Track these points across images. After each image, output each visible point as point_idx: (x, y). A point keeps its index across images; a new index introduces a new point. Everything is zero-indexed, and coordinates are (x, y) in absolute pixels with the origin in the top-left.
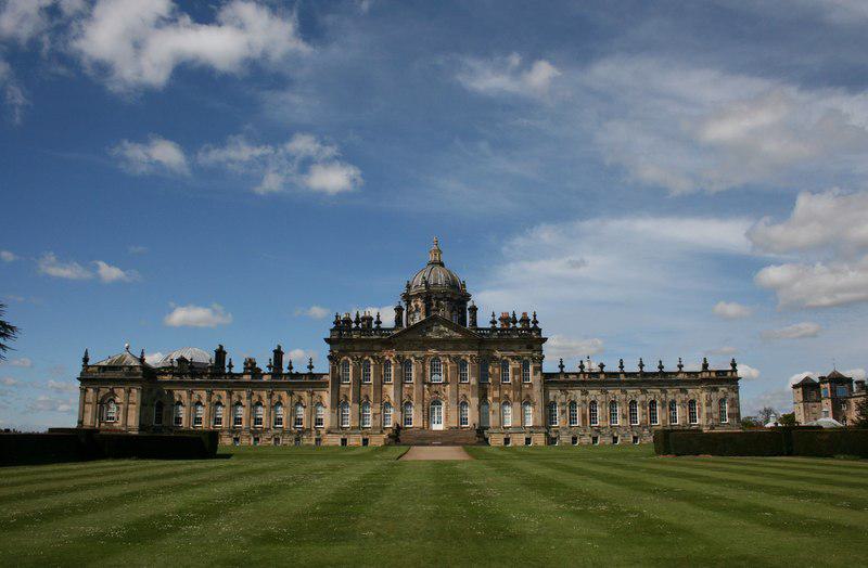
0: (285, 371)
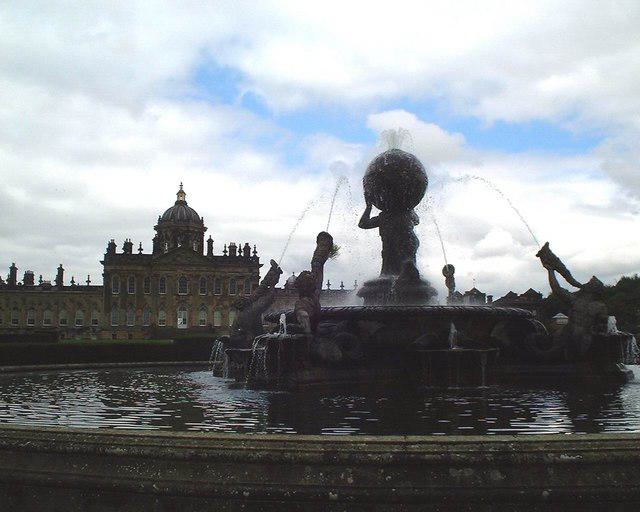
0: (67, 283)
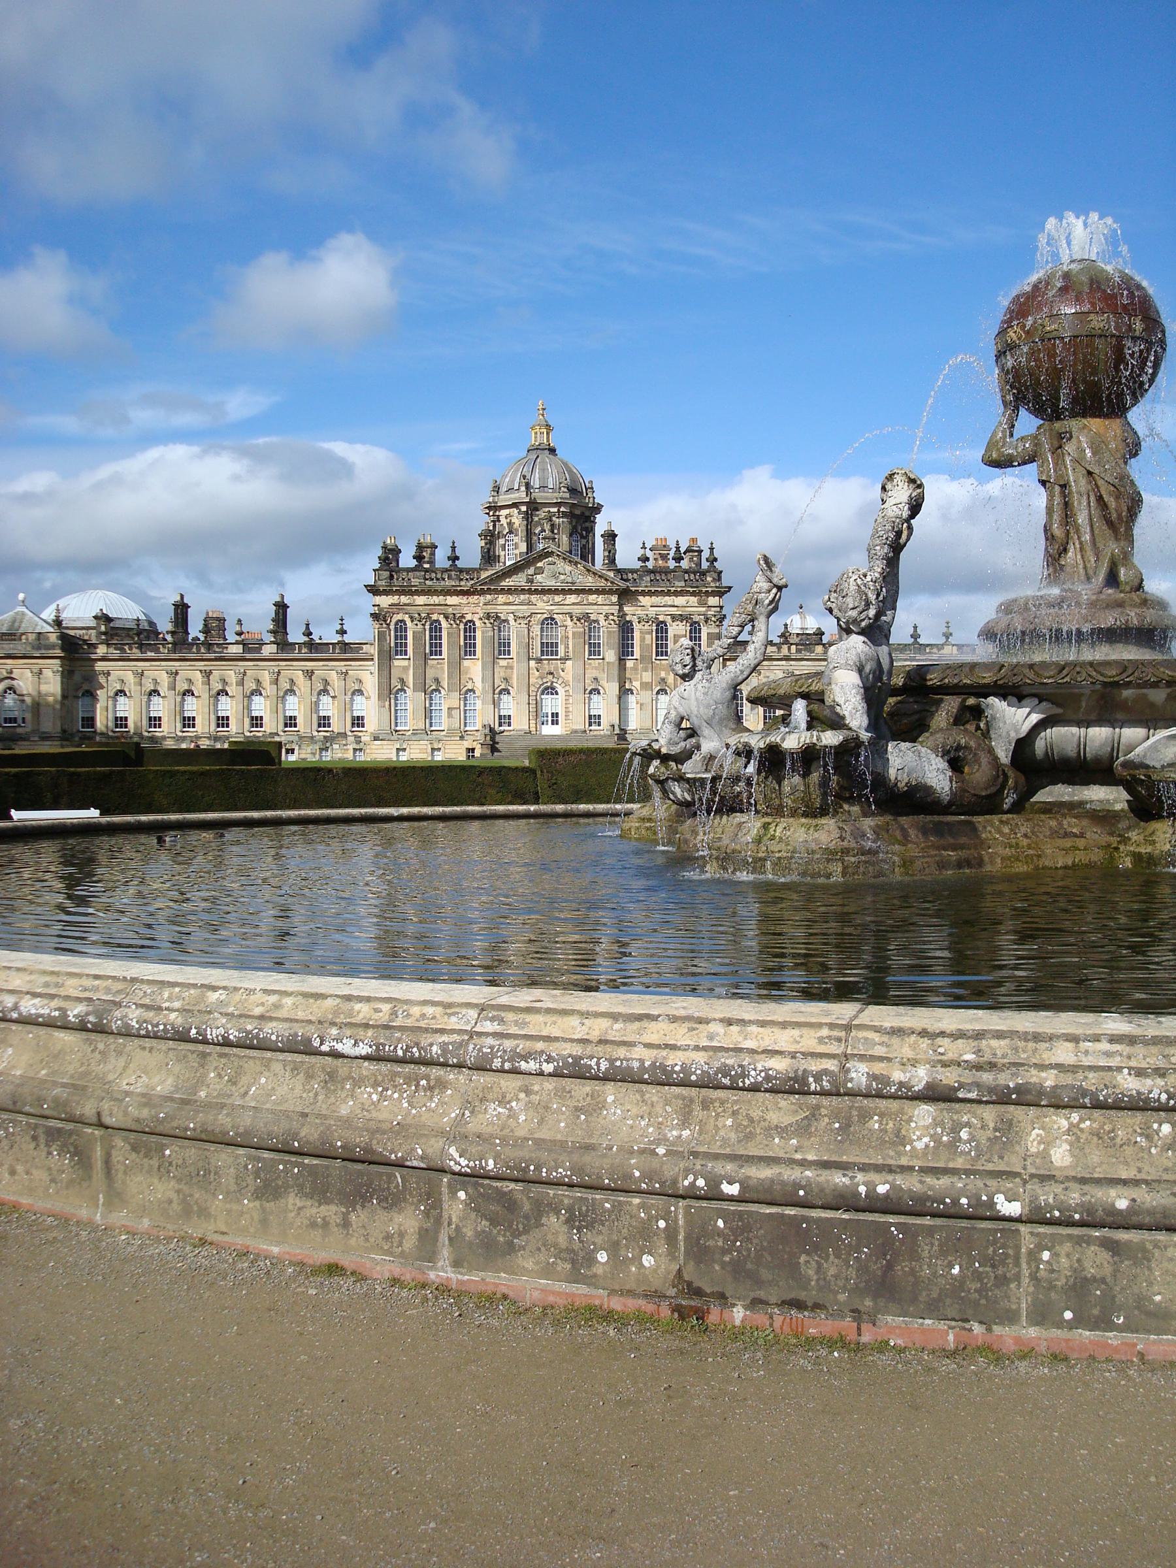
0: (295, 635)
